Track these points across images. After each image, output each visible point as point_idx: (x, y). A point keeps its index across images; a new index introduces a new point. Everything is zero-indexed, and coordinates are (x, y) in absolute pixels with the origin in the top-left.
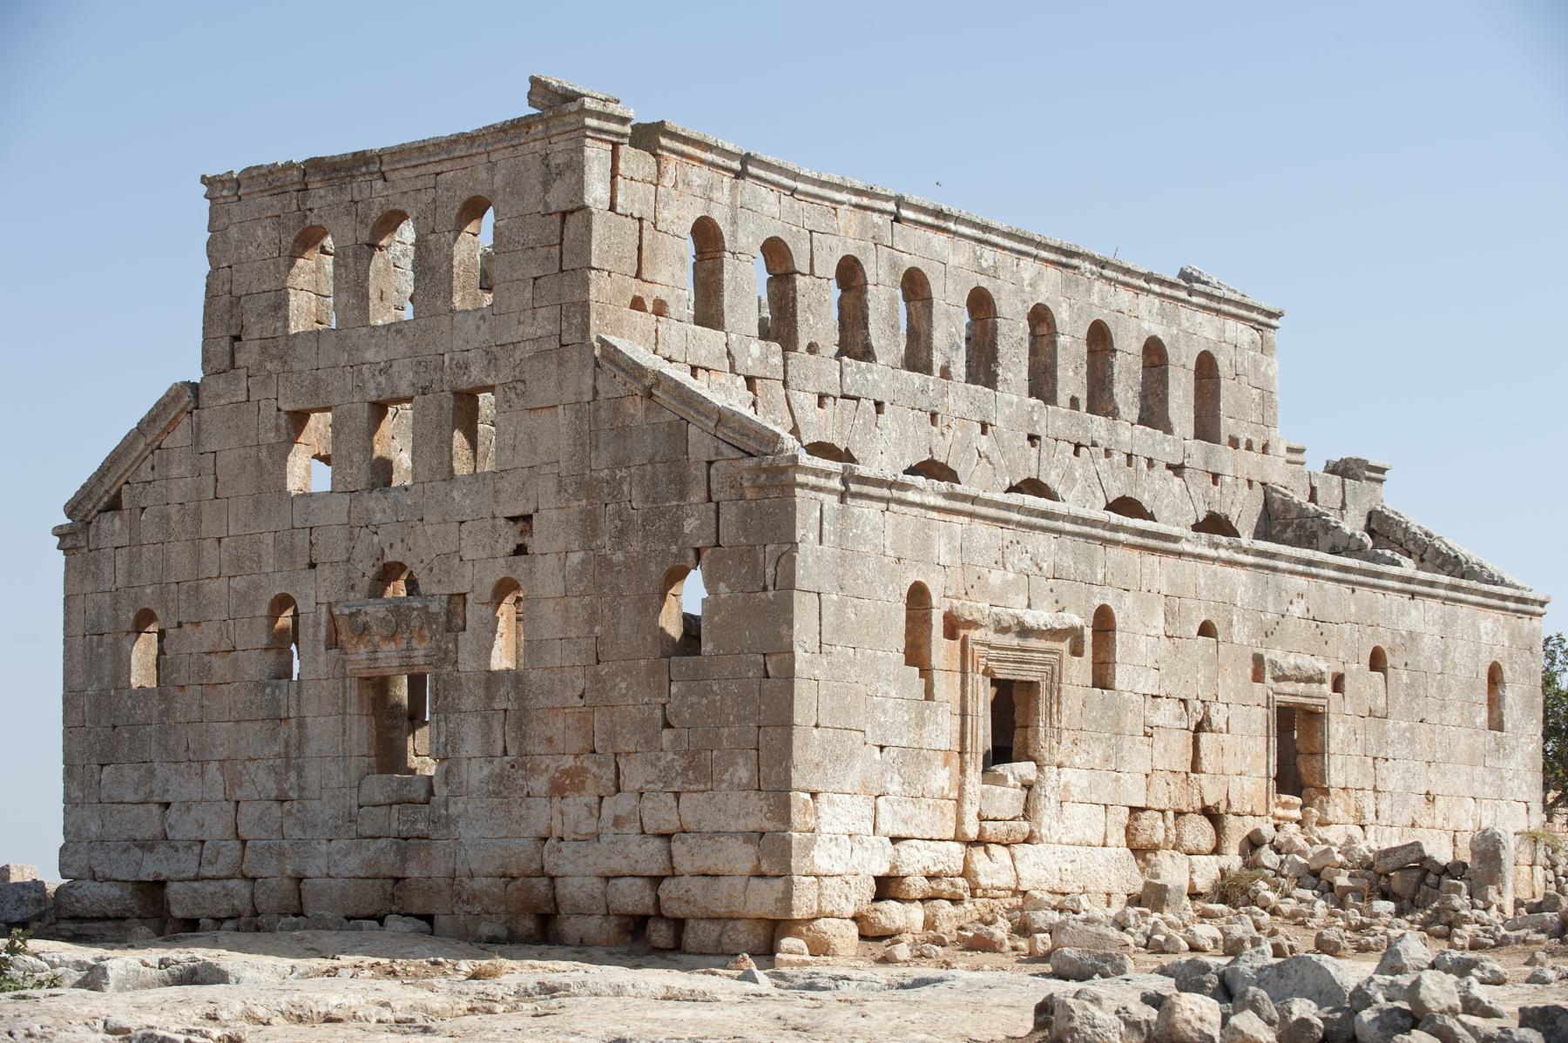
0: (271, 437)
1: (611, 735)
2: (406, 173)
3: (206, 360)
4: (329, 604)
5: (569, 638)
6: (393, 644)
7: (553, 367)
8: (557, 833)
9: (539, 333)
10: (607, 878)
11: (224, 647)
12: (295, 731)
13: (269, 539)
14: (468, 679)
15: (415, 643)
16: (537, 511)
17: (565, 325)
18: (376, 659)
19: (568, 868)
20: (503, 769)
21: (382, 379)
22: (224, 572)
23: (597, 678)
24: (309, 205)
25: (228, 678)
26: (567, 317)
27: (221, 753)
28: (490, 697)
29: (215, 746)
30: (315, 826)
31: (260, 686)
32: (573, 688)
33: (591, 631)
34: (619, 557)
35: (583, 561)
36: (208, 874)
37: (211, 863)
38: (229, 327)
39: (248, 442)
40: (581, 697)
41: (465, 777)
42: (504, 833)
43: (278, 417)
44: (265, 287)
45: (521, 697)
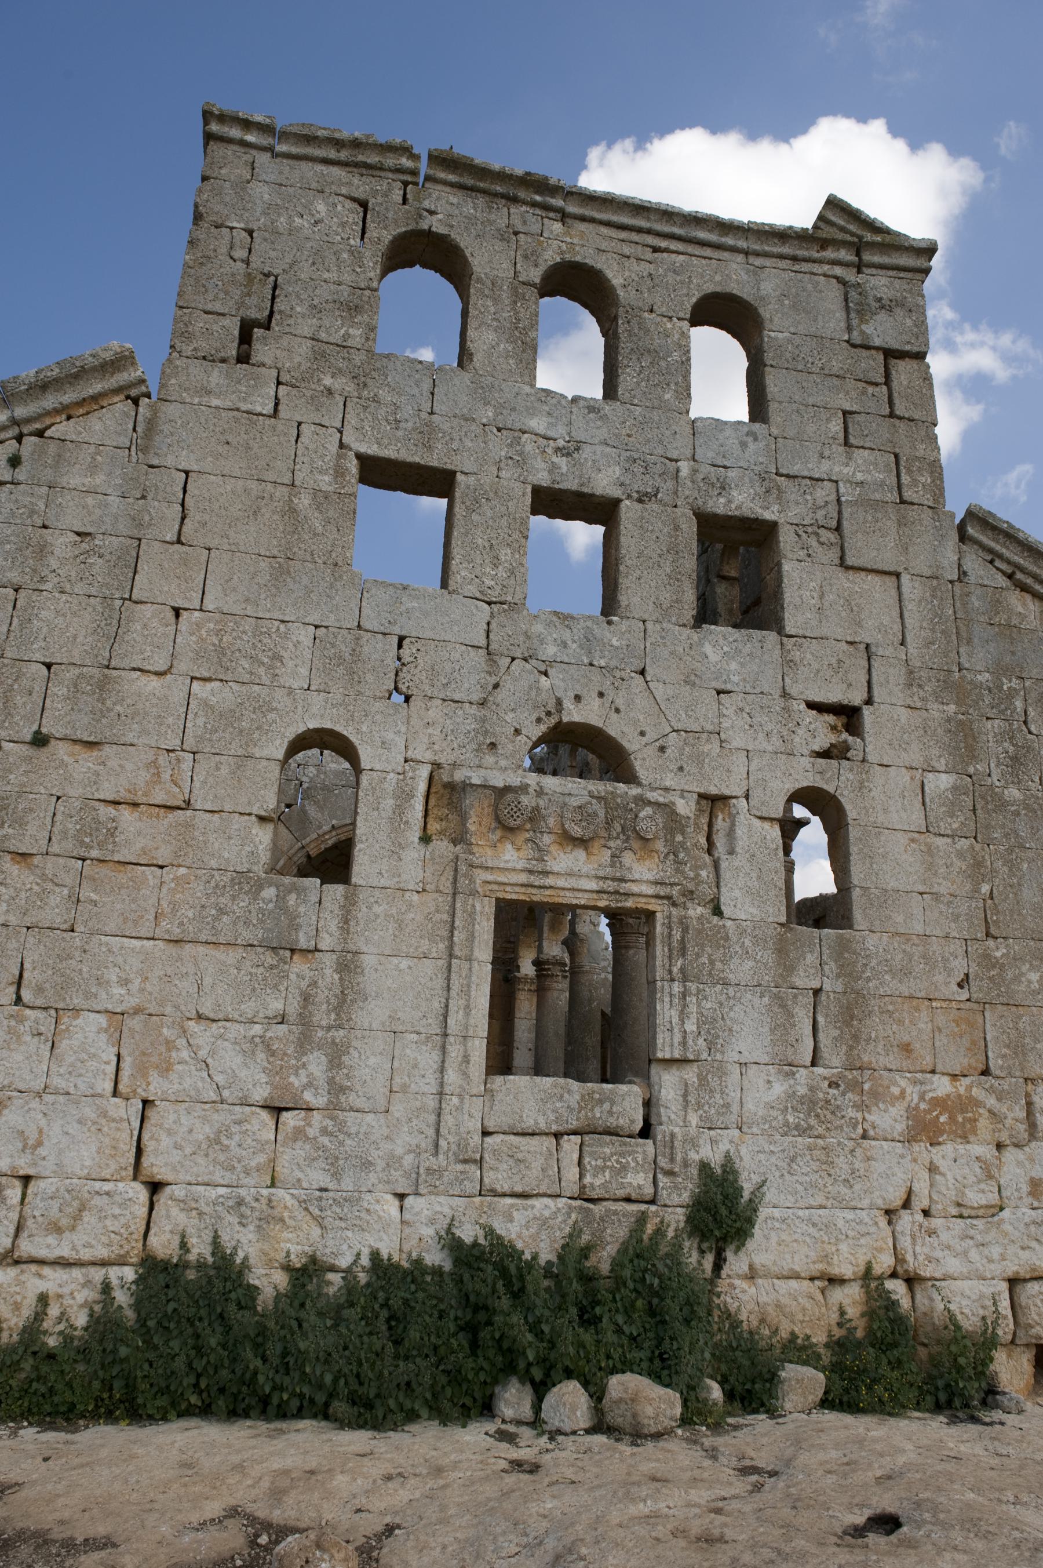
0: (325, 482)
1: (1018, 1049)
2: (604, 230)
3: (182, 333)
4: (436, 766)
5: (936, 896)
6: (580, 854)
7: (891, 525)
8: (921, 1202)
9: (859, 477)
10: (1013, 1282)
11: (159, 798)
12: (330, 975)
13: (304, 635)
14: (743, 933)
15: (628, 858)
16: (869, 702)
17: (905, 479)
18: (546, 873)
19: (953, 1265)
20: (812, 1089)
21: (562, 462)
22: (183, 666)
23: (987, 960)
24: (426, 204)
25: (163, 855)
26: (909, 472)
27: (116, 996)
28: (786, 966)
29: (100, 981)
30: (367, 1165)
31: (243, 881)
32: (949, 971)
33: (977, 890)
34: (1013, 793)
35: (955, 788)
36: (42, 1253)
37: (57, 1229)
38: (240, 305)
39: (271, 476)
40: (960, 985)
41: (734, 1095)
42: (820, 1200)
43: (339, 456)
44: (326, 275)
45: (848, 972)
